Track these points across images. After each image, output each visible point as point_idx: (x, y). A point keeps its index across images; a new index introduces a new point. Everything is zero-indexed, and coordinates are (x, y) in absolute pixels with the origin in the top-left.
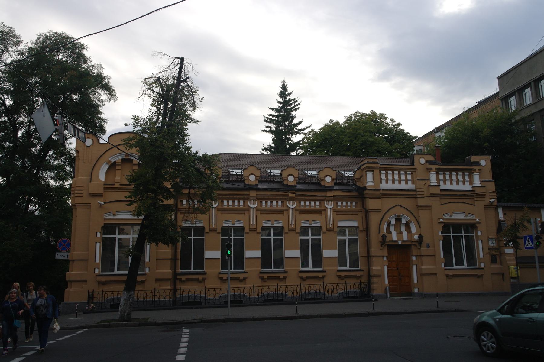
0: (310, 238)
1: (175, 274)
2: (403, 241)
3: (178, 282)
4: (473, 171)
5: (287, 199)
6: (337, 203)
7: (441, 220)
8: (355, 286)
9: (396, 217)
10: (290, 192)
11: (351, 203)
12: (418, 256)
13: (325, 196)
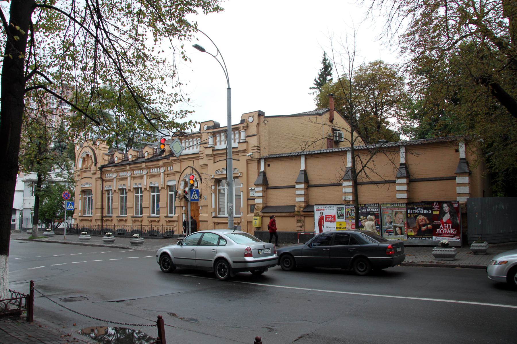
1: (102, 217)
6: (168, 168)
13: (159, 164)
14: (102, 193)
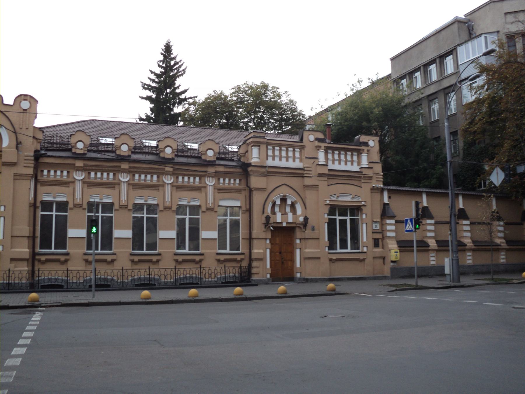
0: (187, 217)
1: (34, 254)
2: (287, 223)
3: (36, 263)
4: (361, 152)
5: (163, 174)
6: (219, 180)
7: (328, 202)
8: (234, 270)
9: (281, 197)
10: (167, 165)
11: (235, 180)
12: (302, 239)
13: (206, 172)
14: (34, 206)
